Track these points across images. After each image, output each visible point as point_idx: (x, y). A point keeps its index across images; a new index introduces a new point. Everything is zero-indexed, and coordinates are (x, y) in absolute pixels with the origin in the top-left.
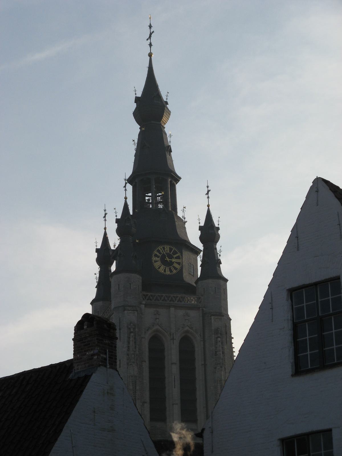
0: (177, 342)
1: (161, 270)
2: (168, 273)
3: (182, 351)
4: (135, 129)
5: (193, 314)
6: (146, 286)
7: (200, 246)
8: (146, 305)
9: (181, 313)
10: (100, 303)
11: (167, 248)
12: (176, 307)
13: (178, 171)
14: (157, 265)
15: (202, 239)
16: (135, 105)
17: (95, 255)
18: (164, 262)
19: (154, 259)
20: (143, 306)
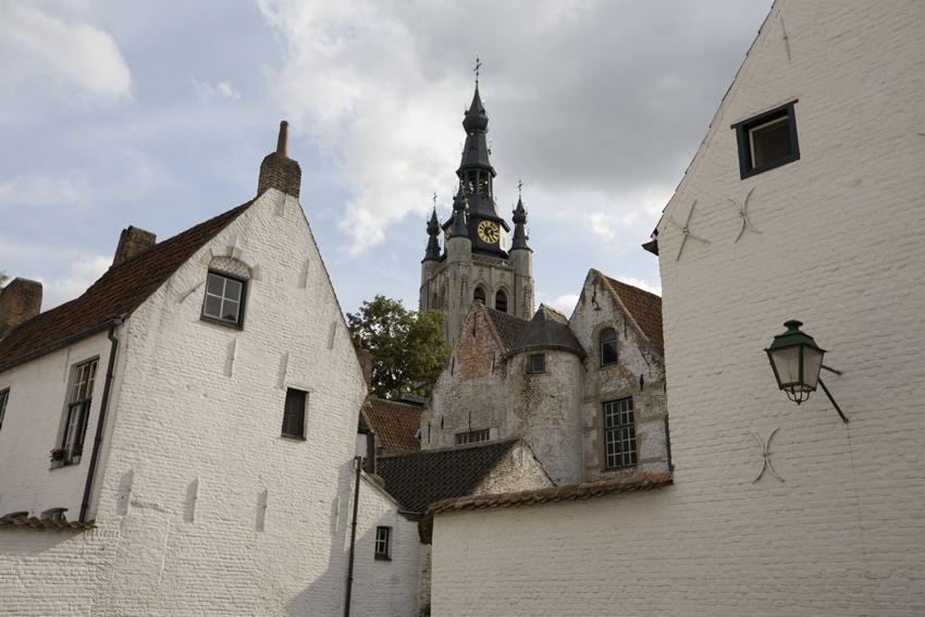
0: (495, 294)
1: (484, 239)
2: (489, 241)
3: (497, 302)
4: (463, 136)
5: (507, 274)
6: (474, 250)
7: (512, 226)
8: (475, 264)
9: (499, 272)
10: (430, 262)
11: (489, 223)
12: (496, 268)
13: (496, 169)
14: (481, 235)
15: (514, 220)
16: (464, 117)
17: (427, 226)
18: (487, 234)
19: (479, 230)
20: (472, 264)
